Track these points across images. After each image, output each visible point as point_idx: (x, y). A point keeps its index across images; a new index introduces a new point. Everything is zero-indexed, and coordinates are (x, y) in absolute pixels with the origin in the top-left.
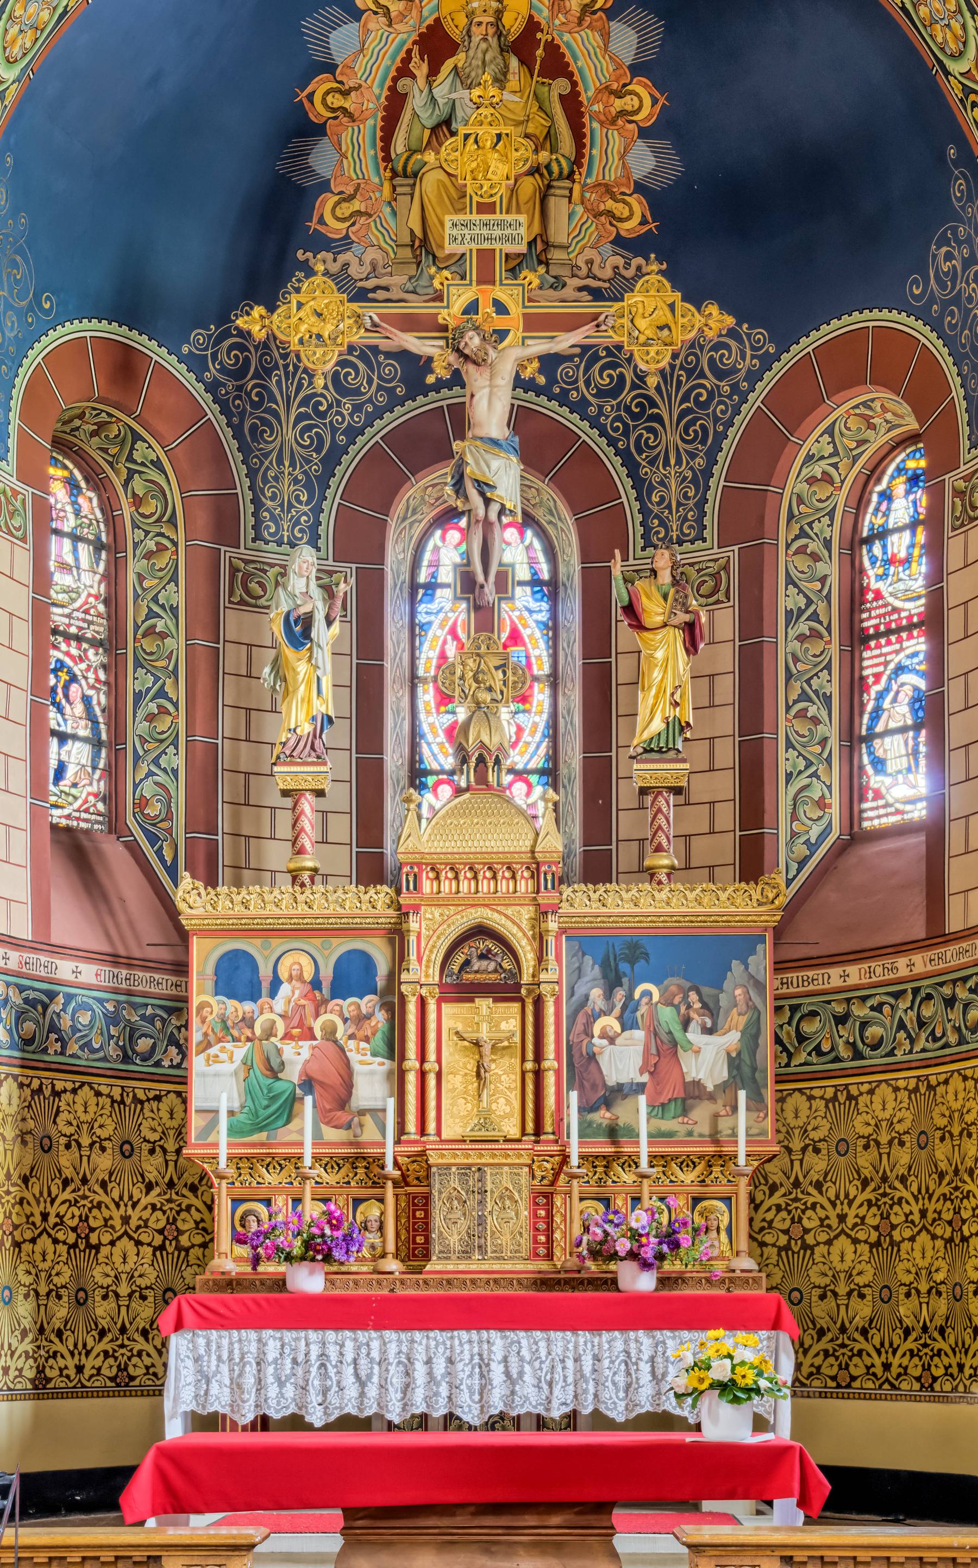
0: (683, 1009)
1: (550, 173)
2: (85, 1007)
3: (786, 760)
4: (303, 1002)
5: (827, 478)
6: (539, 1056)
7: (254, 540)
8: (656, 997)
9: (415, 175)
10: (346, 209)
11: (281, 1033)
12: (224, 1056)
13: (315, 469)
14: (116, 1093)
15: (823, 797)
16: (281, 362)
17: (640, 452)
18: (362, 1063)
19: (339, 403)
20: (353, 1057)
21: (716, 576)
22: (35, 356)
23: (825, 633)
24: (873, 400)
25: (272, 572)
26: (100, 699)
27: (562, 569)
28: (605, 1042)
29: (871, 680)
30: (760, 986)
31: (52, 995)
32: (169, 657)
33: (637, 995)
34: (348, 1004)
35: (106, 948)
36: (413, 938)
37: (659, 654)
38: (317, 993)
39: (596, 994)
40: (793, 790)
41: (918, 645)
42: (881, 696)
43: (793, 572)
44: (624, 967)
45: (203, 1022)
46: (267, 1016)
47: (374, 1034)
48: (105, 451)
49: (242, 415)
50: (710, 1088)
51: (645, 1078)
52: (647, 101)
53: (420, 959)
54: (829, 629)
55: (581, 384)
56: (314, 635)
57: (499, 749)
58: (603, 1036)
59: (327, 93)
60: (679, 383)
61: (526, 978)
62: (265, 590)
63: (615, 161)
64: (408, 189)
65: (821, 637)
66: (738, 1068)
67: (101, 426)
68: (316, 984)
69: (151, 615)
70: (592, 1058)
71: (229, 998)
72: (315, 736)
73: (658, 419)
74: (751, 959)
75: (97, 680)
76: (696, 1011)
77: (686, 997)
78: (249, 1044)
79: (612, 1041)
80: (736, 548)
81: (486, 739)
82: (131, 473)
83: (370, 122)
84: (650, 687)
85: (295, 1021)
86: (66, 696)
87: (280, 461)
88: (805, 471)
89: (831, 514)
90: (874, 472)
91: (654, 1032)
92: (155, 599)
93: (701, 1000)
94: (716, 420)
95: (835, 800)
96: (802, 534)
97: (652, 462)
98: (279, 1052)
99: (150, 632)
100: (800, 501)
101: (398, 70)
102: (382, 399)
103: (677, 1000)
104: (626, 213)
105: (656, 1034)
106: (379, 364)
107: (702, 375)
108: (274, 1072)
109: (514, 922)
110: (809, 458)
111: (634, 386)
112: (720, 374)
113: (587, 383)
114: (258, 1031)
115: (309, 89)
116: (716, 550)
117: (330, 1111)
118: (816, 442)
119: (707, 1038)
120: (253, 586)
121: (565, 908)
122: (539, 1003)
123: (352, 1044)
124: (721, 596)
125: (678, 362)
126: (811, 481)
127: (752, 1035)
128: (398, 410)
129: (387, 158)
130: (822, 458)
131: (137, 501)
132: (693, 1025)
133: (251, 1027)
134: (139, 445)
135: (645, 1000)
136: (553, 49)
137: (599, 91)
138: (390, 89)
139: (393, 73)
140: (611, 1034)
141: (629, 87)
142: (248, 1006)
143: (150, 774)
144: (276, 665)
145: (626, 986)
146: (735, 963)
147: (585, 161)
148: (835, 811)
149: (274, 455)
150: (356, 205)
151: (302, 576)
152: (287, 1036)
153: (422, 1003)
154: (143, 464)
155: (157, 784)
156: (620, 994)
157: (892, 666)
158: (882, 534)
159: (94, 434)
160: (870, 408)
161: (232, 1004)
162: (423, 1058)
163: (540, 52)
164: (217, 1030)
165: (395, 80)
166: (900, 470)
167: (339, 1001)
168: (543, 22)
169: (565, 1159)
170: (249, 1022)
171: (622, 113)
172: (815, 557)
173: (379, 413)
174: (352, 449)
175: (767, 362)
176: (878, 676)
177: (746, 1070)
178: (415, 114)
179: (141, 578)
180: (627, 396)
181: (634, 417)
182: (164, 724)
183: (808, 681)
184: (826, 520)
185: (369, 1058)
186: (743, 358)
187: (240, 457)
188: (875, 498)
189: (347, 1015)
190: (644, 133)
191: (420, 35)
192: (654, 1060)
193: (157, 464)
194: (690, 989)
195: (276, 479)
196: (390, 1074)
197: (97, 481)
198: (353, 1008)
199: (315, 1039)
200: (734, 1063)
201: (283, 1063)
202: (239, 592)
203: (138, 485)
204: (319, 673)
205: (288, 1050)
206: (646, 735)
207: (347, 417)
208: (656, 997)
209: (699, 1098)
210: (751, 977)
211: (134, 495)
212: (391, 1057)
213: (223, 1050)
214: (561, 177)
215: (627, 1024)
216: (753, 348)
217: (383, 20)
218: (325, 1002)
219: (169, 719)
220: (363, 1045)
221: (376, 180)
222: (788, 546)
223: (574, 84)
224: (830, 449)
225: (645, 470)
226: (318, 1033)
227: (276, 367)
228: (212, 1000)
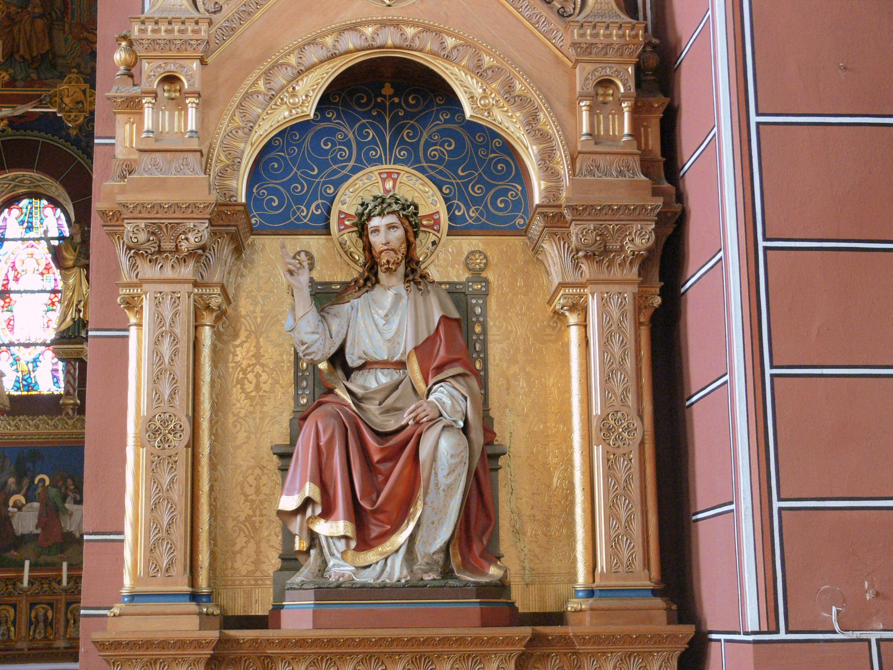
0: (63, 490)
1: (52, 18)
8: (47, 483)
28: (15, 510)
33: (36, 482)
58: (15, 505)
77: (65, 482)
79: (20, 509)
103: (60, 484)
132: (69, 499)
135: (41, 484)
140: (20, 505)
147: (69, 11)
156: (26, 481)
208: (47, 483)
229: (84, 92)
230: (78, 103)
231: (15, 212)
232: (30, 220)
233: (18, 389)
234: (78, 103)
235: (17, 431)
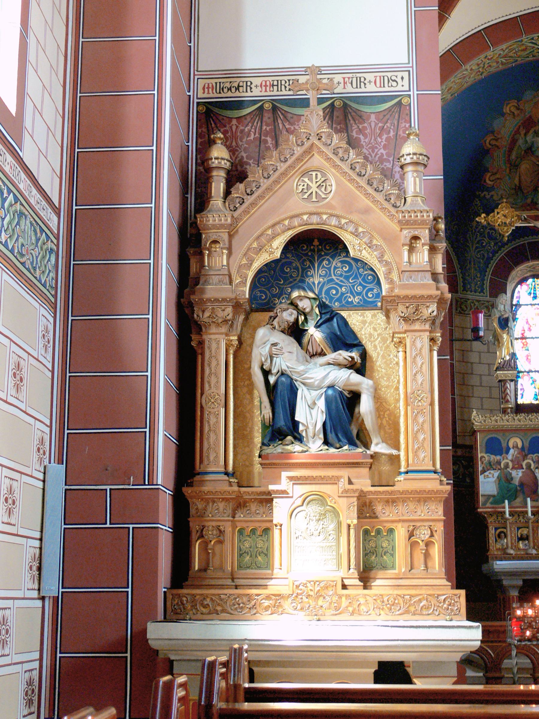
4: (518, 456)
7: (463, 291)
9: (517, 166)
12: (490, 476)
25: (469, 302)
45: (482, 463)
46: (506, 461)
56: (509, 325)
62: (467, 308)
64: (515, 170)
68: (523, 448)
78: (499, 471)
83: (504, 149)
85: (516, 463)
87: (470, 263)
98: (511, 474)
101: (515, 132)
114: (502, 466)
120: (463, 307)
133: (500, 464)
138: (512, 138)
139: (513, 133)
142: (498, 457)
150: (498, 176)
152: (513, 468)
161: (492, 457)
165: (514, 135)
167: (532, 455)
170: (499, 463)
174: (494, 258)
178: (519, 146)
198: (536, 458)
199: (523, 469)
202: (459, 309)
205: (514, 473)
207: (492, 248)
213: (490, 473)
221: (504, 167)
226: (524, 467)
228: (485, 455)
231: (524, 287)
232: (535, 292)
233: (537, 399)
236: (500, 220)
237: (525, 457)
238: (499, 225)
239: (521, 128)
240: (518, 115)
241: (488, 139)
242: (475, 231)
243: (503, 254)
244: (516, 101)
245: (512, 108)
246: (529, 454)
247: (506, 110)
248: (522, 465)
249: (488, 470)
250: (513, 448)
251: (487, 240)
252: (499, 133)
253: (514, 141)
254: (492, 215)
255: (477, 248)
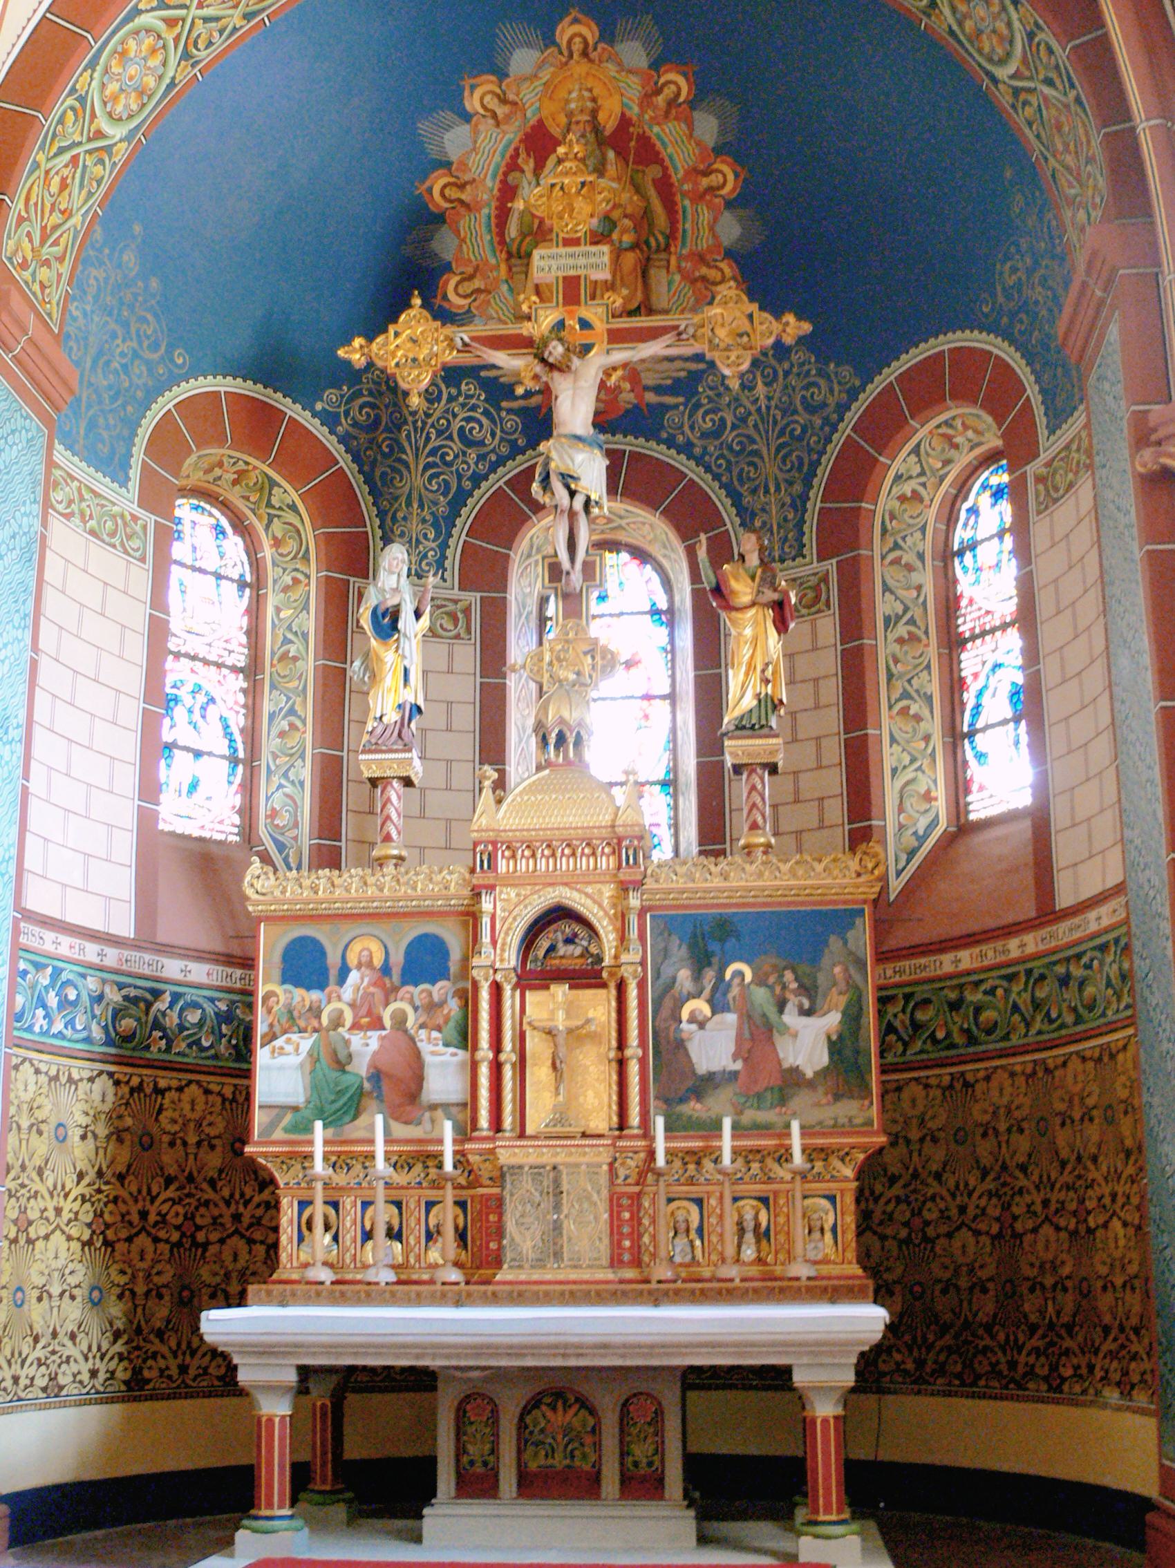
0: (778, 990)
2: (195, 1005)
3: (890, 756)
4: (372, 989)
5: (916, 496)
6: (622, 1044)
10: (467, 288)
11: (348, 1023)
12: (289, 1048)
13: (442, 509)
14: (228, 1090)
15: (928, 792)
16: (410, 419)
17: (742, 483)
18: (433, 1053)
19: (464, 454)
20: (424, 1047)
21: (817, 588)
22: (166, 403)
23: (923, 637)
24: (953, 418)
26: (238, 721)
27: (677, 598)
28: (694, 1027)
29: (969, 681)
30: (861, 964)
31: (157, 994)
32: (300, 678)
33: (728, 976)
34: (418, 991)
35: (219, 947)
36: (486, 921)
37: (748, 632)
38: (387, 980)
39: (684, 976)
40: (899, 783)
41: (1013, 640)
42: (980, 694)
43: (891, 583)
44: (714, 946)
45: (269, 1011)
46: (335, 1005)
47: (446, 1022)
48: (247, 499)
49: (373, 464)
50: (809, 1074)
51: (738, 1066)
52: (731, 177)
53: (494, 942)
54: (926, 633)
55: (686, 429)
56: (400, 625)
57: (579, 724)
58: (692, 1020)
59: (445, 186)
60: (775, 423)
61: (607, 961)
63: (705, 232)
65: (919, 640)
66: (839, 1052)
67: (241, 473)
68: (386, 970)
69: (287, 641)
70: (680, 1045)
71: (296, 986)
72: (402, 724)
73: (756, 453)
74: (850, 935)
75: (236, 703)
76: (793, 991)
79: (702, 1025)
80: (834, 561)
81: (566, 715)
82: (271, 518)
83: (485, 211)
84: (740, 664)
85: (364, 1011)
86: (204, 717)
88: (894, 490)
89: (923, 529)
90: (962, 489)
91: (747, 1017)
92: (289, 628)
93: (796, 979)
94: (810, 450)
95: (940, 793)
96: (896, 546)
97: (754, 491)
98: (347, 1043)
99: (284, 657)
100: (892, 517)
101: (508, 165)
102: (504, 450)
103: (772, 980)
104: (718, 276)
105: (749, 1017)
106: (501, 419)
107: (795, 412)
108: (341, 1063)
109: (595, 902)
110: (898, 478)
111: (734, 427)
112: (811, 409)
113: (692, 428)
114: (325, 1020)
115: (428, 184)
116: (815, 564)
117: (400, 1106)
118: (902, 462)
119: (805, 1020)
121: (650, 884)
122: (621, 987)
123: (423, 1034)
124: (821, 605)
125: (773, 403)
126: (902, 498)
127: (853, 1017)
128: (520, 458)
129: (502, 242)
130: (910, 477)
131: (277, 543)
132: (790, 1008)
133: (318, 1017)
134: (276, 490)
135: (737, 981)
136: (644, 141)
137: (687, 173)
140: (700, 1018)
141: (715, 166)
142: (315, 995)
143: (280, 786)
144: (367, 656)
145: (716, 967)
146: (833, 939)
148: (941, 805)
149: (403, 499)
150: (477, 283)
151: (392, 573)
152: (356, 1026)
153: (497, 989)
154: (280, 509)
155: (287, 796)
156: (710, 975)
157: (989, 666)
158: (973, 546)
159: (235, 482)
160: (951, 426)
161: (298, 993)
162: (497, 1046)
163: (633, 144)
164: (283, 1021)
165: (505, 174)
166: (984, 487)
167: (410, 988)
168: (635, 119)
169: (651, 1154)
170: (316, 1012)
171: (711, 190)
172: (910, 568)
173: (501, 461)
174: (477, 493)
175: (853, 394)
176: (976, 675)
177: (848, 1052)
179: (278, 610)
180: (729, 436)
181: (737, 454)
182: (293, 741)
183: (909, 681)
184: (918, 535)
185: (441, 1048)
186: (832, 391)
187: (370, 499)
188: (963, 515)
189: (418, 1003)
190: (729, 205)
191: (526, 135)
192: (747, 1045)
193: (293, 507)
194: (785, 968)
195: (405, 518)
196: (462, 1064)
197: (241, 527)
199: (383, 1028)
200: (835, 1047)
201: (350, 1056)
203: (277, 527)
204: (406, 663)
205: (356, 1040)
206: (737, 713)
209: (798, 1085)
210: (851, 953)
211: (275, 538)
212: (465, 1048)
213: (288, 1041)
214: (658, 251)
215: (717, 1007)
216: (839, 383)
217: (491, 121)
218: (395, 989)
219: (297, 735)
220: (435, 1034)
221: (493, 261)
222: (883, 558)
223: (665, 169)
224: (917, 469)
225: (747, 500)
226: (387, 1022)
227: (406, 422)
228: (279, 990)
229: (750, 317)
230: (741, 335)
234: (741, 335)
235: (691, 885)
236: (400, 353)
237: (390, 994)
238: (397, 365)
239: (523, 155)
240: (508, 117)
241: (438, 182)
242: (424, 423)
243: (501, 483)
244: (493, 78)
245: (488, 98)
246: (404, 983)
247: (473, 103)
248: (380, 1019)
249: (285, 1032)
250: (359, 967)
251: (457, 446)
252: (463, 165)
253: (508, 192)
254: (380, 339)
255: (428, 466)
